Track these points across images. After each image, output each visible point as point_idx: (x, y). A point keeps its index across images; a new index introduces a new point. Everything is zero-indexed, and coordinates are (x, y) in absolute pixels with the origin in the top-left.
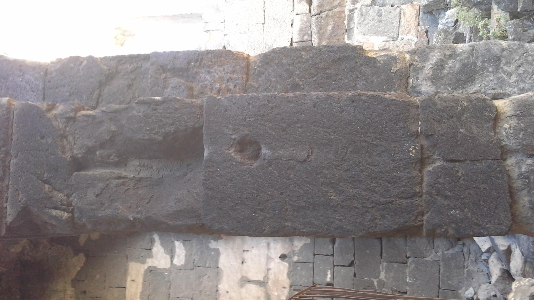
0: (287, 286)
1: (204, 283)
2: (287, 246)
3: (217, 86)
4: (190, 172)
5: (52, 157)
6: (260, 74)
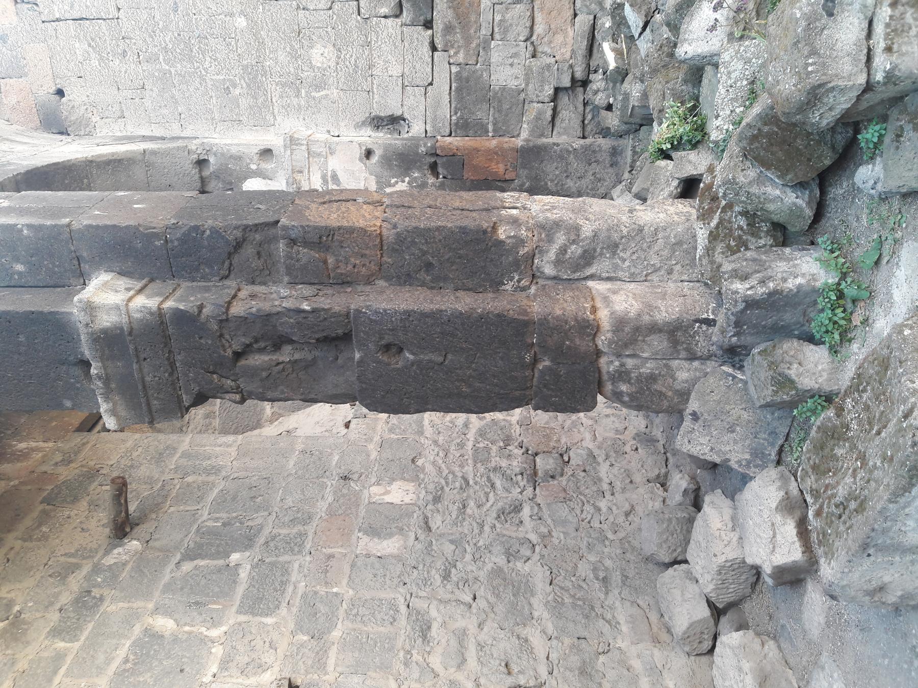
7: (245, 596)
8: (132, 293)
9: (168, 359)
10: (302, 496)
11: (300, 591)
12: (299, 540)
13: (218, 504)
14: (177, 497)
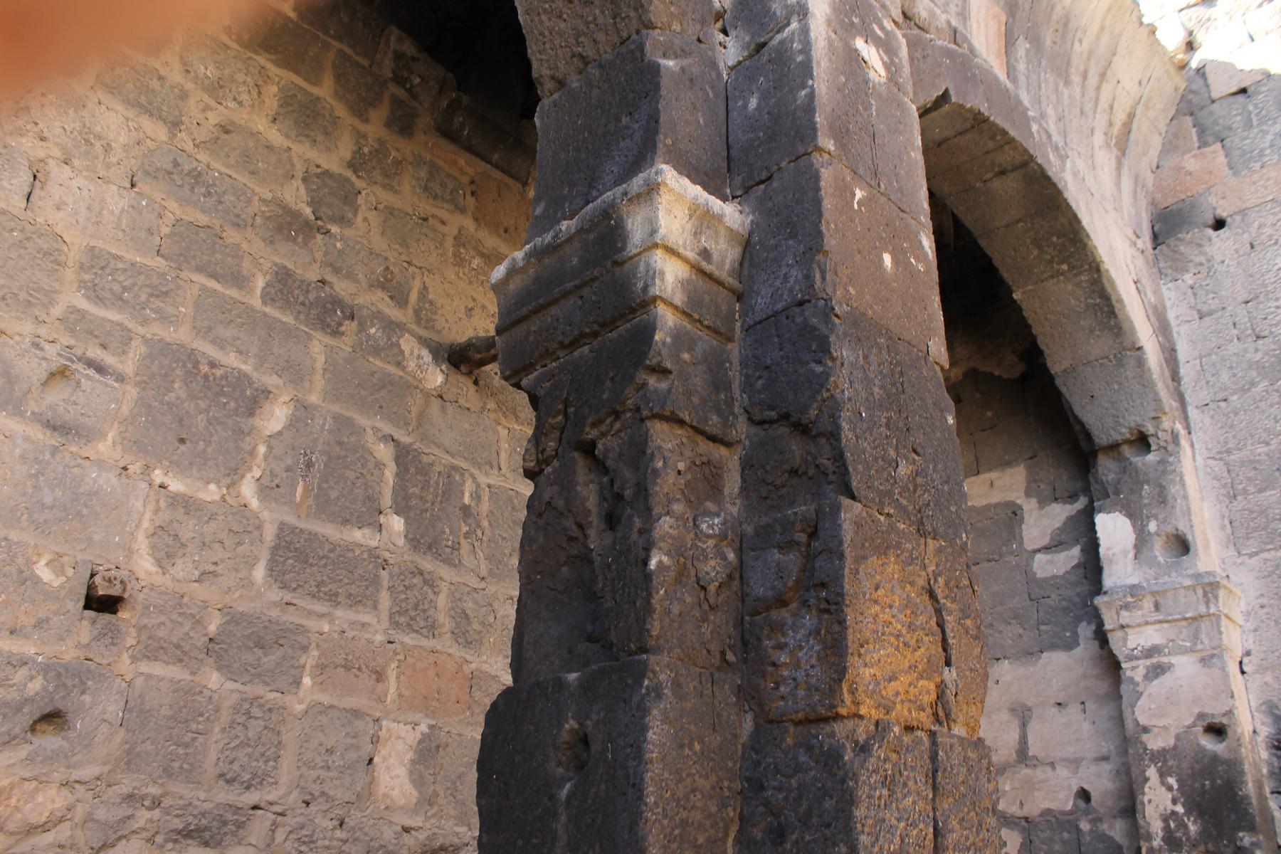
0: (1025, 812)
1: (1009, 628)
2: (1109, 803)
3: (784, 658)
4: (603, 647)
6: (809, 748)
7: (313, 537)
8: (691, 255)
9: (583, 335)
11: (312, 624)
12: (422, 624)
13: (510, 499)
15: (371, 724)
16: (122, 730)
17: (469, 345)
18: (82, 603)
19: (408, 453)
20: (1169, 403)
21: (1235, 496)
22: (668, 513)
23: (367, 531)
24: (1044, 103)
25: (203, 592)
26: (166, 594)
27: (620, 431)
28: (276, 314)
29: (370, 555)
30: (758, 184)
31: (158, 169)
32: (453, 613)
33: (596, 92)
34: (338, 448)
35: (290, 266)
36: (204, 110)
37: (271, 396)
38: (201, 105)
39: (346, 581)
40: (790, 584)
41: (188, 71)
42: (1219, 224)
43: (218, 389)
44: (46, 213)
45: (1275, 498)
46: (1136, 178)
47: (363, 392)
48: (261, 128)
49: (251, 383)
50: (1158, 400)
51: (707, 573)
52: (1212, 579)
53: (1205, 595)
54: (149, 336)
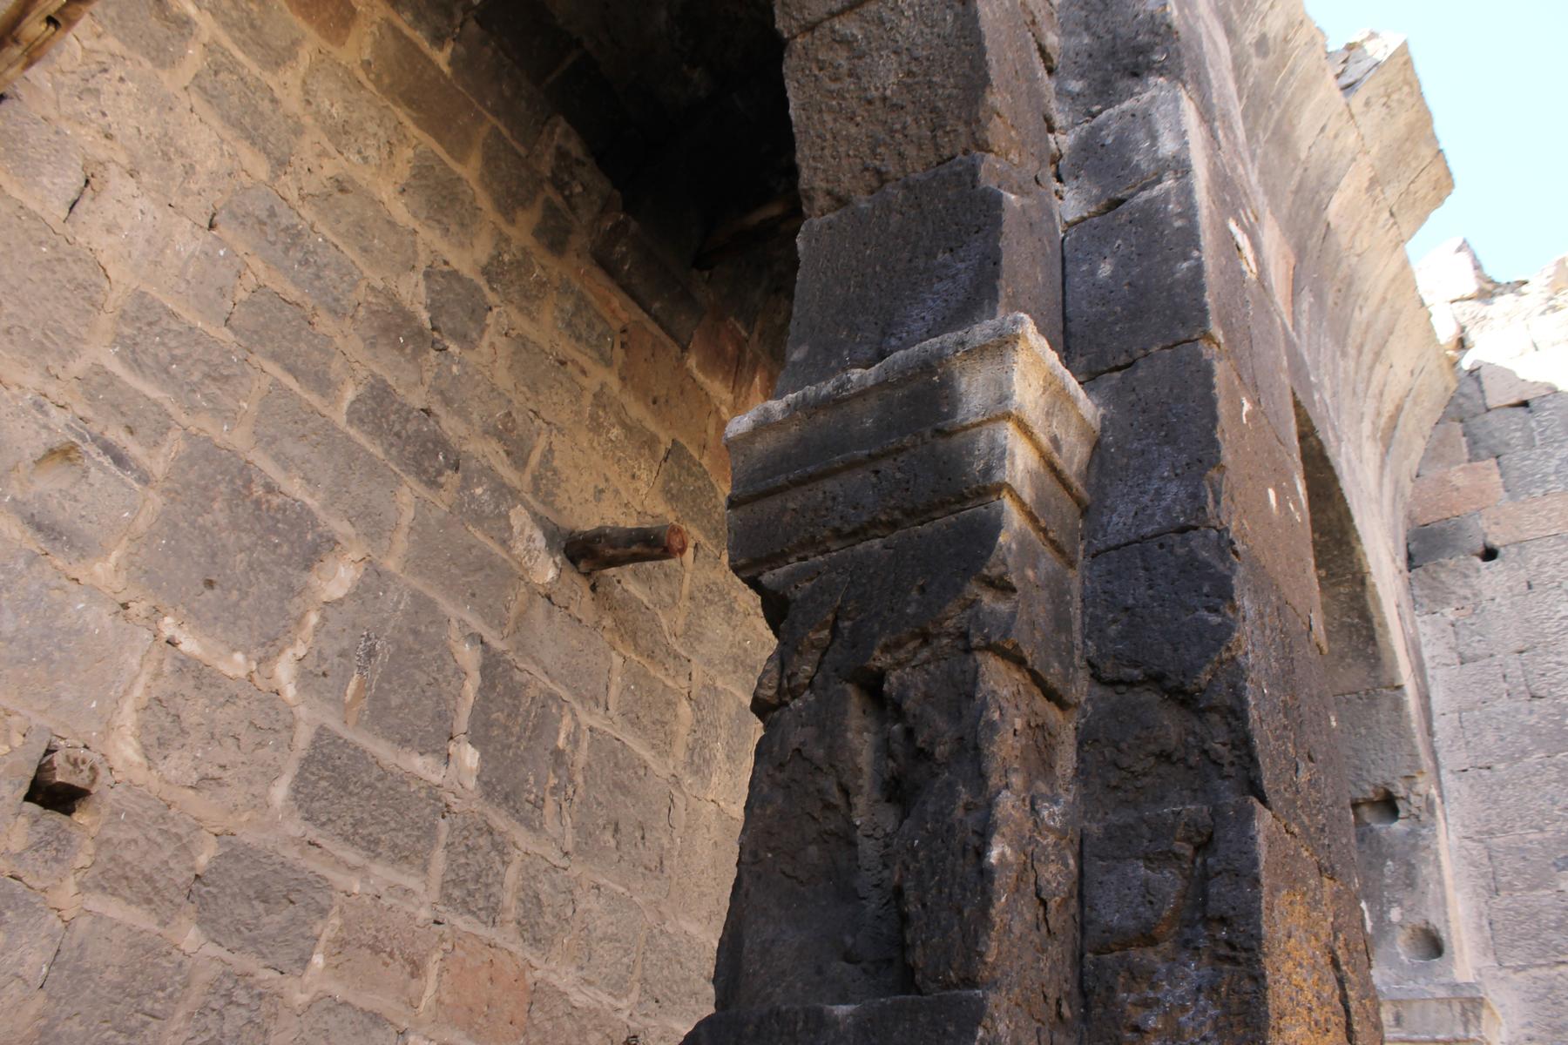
4: (865, 971)
5: (877, 627)
7: (359, 754)
8: (1044, 440)
9: (874, 523)
10: (599, 933)
11: (338, 878)
13: (614, 752)
14: (646, 675)
15: (394, 1037)
16: (43, 993)
17: (599, 535)
18: (24, 791)
19: (498, 662)
20: (1426, 762)
21: (1497, 890)
22: (1007, 786)
23: (430, 760)
24: (1322, 371)
25: (198, 805)
26: (147, 798)
27: (928, 662)
28: (362, 439)
29: (430, 795)
30: (1111, 370)
31: (247, 214)
32: (522, 894)
33: (895, 218)
34: (411, 638)
35: (391, 382)
36: (319, 156)
37: (338, 548)
38: (317, 149)
39: (393, 825)
40: (1166, 913)
41: (309, 102)
42: (1490, 554)
43: (270, 523)
44: (91, 234)
45: (1548, 900)
46: (1396, 483)
47: (454, 570)
48: (385, 197)
49: (315, 525)
50: (1414, 755)
51: (1049, 882)
52: (1474, 994)
53: (1464, 1013)
54: (193, 430)
